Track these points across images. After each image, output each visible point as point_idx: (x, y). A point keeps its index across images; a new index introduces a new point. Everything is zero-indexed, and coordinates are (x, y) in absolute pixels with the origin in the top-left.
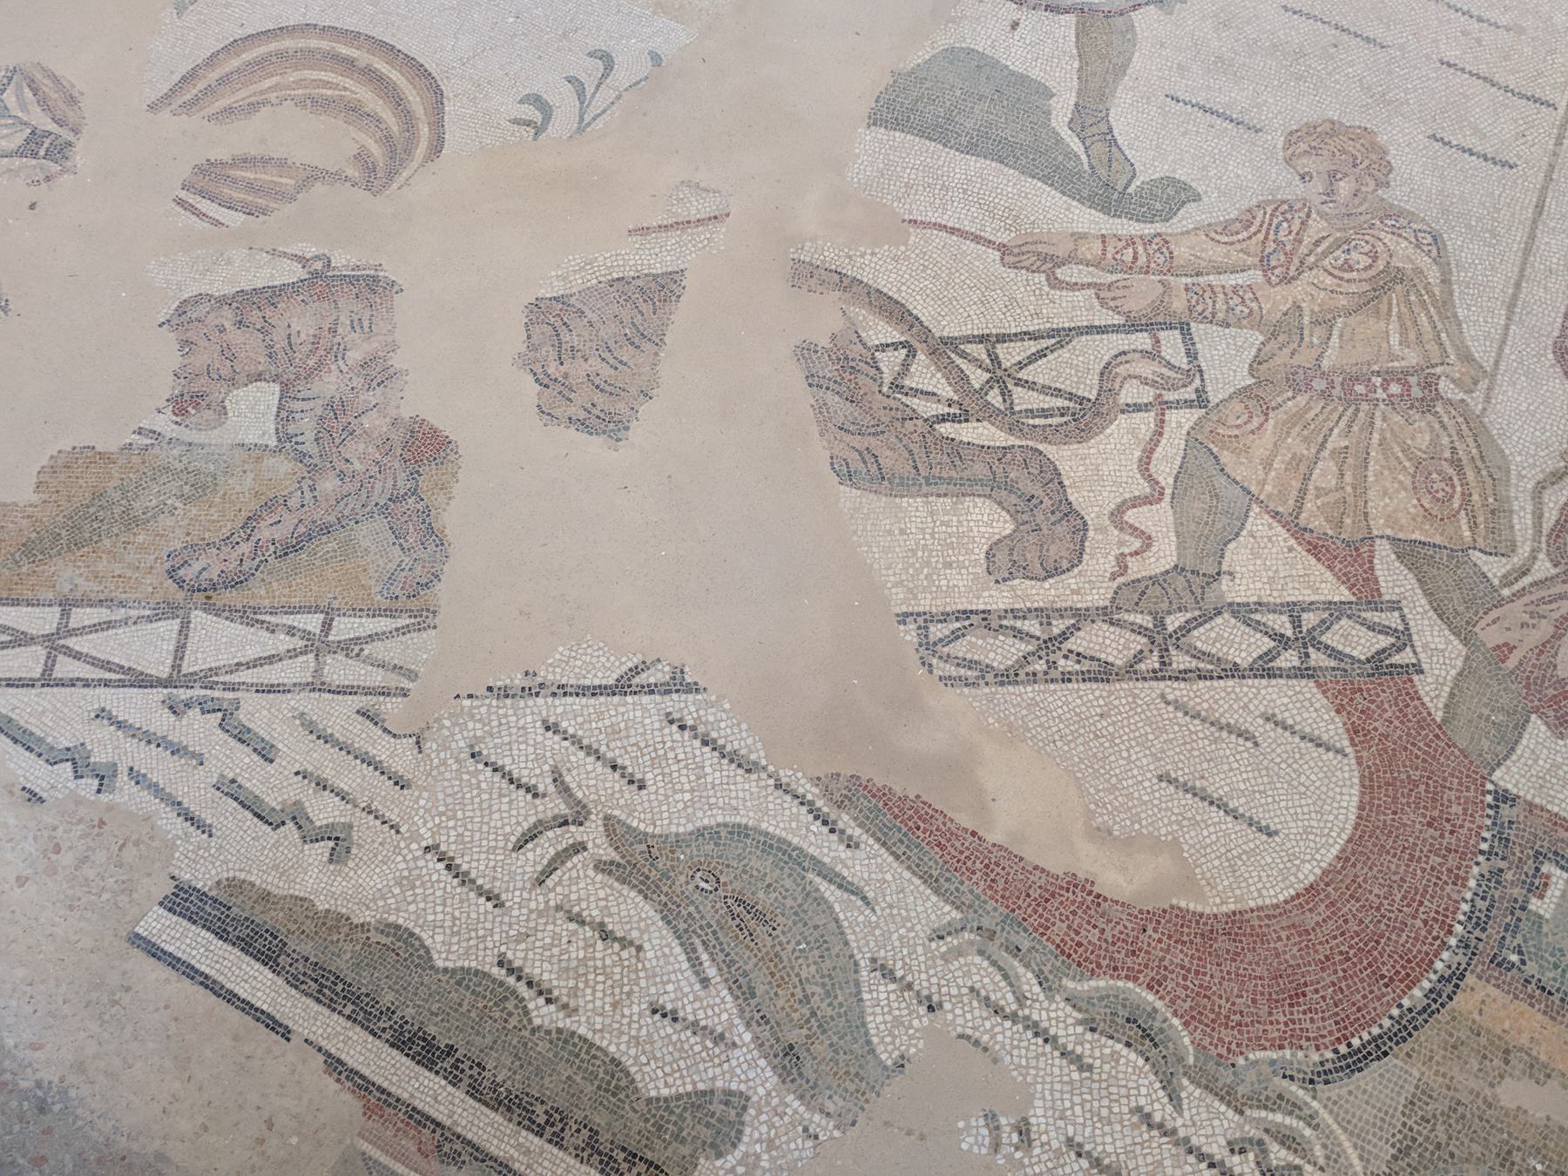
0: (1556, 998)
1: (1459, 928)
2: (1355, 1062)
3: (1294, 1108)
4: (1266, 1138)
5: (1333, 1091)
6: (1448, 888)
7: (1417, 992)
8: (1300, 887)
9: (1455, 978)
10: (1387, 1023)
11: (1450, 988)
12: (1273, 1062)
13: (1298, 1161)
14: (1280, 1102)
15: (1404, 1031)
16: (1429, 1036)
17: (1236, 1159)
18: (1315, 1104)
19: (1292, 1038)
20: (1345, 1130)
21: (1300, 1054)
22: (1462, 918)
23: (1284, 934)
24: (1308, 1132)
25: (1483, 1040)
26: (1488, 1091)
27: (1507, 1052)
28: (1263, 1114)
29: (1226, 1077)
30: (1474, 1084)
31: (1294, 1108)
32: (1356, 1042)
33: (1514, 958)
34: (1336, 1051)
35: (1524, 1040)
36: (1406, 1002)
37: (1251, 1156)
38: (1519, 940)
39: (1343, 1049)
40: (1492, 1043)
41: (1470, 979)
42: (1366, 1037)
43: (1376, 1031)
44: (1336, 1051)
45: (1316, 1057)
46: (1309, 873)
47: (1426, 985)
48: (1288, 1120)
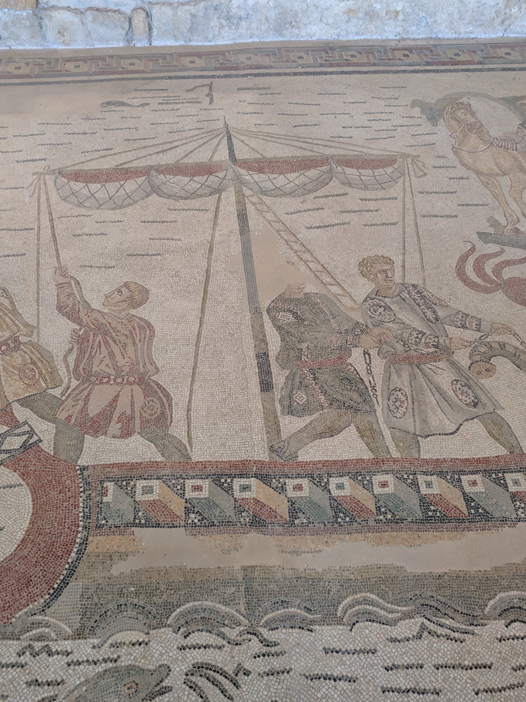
0: (122, 527)
1: (81, 523)
2: (57, 593)
3: (39, 624)
4: (31, 642)
5: (52, 609)
6: (73, 511)
7: (73, 555)
8: (18, 542)
9: (85, 540)
10: (65, 572)
11: (84, 546)
12: (26, 613)
13: (46, 643)
14: (34, 625)
15: (72, 572)
16: (82, 568)
17: (22, 658)
18: (47, 618)
19: (32, 599)
20: (60, 620)
21: (36, 603)
22: (81, 519)
23: (17, 563)
24: (47, 630)
25: (101, 557)
26: (108, 574)
27: (111, 556)
28: (28, 634)
29: (10, 629)
30: (102, 575)
31: (39, 624)
32: (56, 586)
33: (103, 522)
34: (49, 594)
35: (115, 548)
36: (70, 561)
37: (28, 653)
38: (103, 514)
39: (52, 591)
40: (104, 556)
41: (90, 539)
42: (59, 582)
43: (62, 577)
44: (49, 594)
45: (42, 601)
46: (20, 535)
47: (75, 550)
48: (38, 631)
